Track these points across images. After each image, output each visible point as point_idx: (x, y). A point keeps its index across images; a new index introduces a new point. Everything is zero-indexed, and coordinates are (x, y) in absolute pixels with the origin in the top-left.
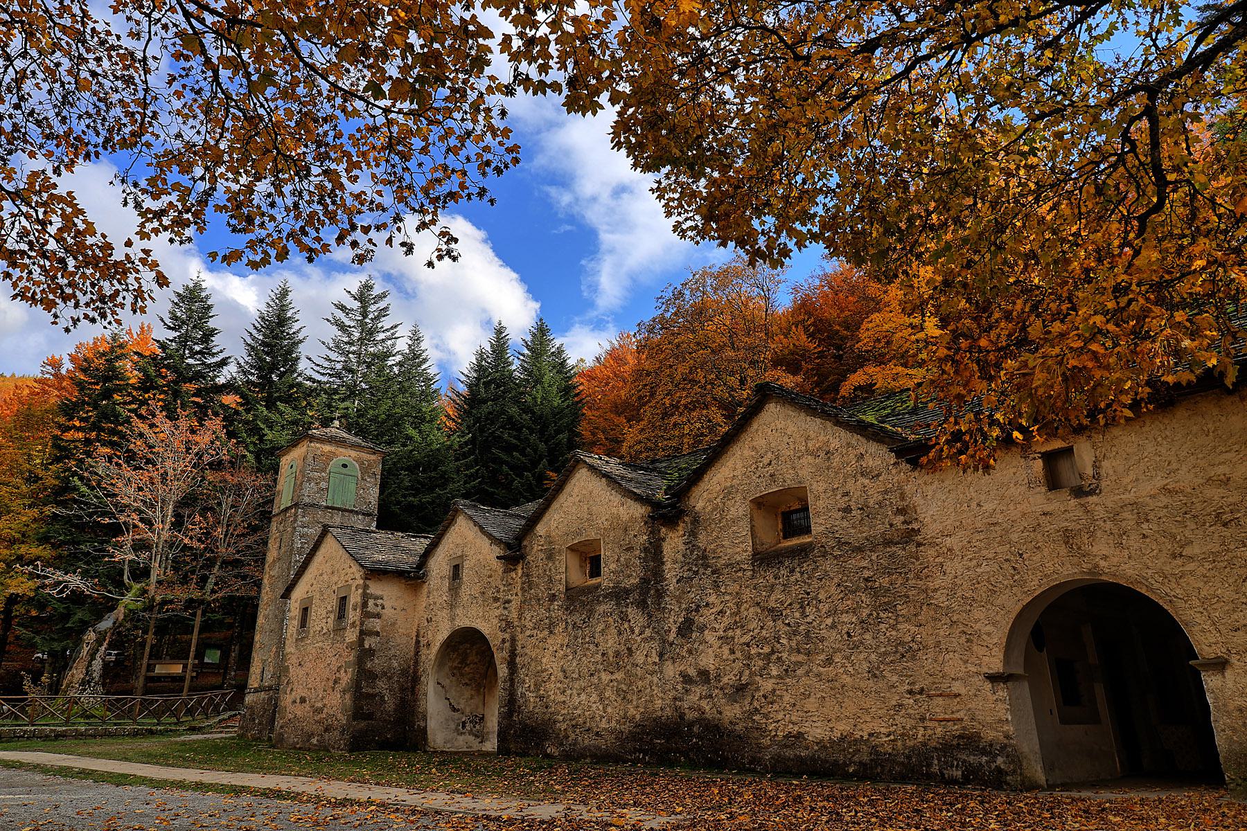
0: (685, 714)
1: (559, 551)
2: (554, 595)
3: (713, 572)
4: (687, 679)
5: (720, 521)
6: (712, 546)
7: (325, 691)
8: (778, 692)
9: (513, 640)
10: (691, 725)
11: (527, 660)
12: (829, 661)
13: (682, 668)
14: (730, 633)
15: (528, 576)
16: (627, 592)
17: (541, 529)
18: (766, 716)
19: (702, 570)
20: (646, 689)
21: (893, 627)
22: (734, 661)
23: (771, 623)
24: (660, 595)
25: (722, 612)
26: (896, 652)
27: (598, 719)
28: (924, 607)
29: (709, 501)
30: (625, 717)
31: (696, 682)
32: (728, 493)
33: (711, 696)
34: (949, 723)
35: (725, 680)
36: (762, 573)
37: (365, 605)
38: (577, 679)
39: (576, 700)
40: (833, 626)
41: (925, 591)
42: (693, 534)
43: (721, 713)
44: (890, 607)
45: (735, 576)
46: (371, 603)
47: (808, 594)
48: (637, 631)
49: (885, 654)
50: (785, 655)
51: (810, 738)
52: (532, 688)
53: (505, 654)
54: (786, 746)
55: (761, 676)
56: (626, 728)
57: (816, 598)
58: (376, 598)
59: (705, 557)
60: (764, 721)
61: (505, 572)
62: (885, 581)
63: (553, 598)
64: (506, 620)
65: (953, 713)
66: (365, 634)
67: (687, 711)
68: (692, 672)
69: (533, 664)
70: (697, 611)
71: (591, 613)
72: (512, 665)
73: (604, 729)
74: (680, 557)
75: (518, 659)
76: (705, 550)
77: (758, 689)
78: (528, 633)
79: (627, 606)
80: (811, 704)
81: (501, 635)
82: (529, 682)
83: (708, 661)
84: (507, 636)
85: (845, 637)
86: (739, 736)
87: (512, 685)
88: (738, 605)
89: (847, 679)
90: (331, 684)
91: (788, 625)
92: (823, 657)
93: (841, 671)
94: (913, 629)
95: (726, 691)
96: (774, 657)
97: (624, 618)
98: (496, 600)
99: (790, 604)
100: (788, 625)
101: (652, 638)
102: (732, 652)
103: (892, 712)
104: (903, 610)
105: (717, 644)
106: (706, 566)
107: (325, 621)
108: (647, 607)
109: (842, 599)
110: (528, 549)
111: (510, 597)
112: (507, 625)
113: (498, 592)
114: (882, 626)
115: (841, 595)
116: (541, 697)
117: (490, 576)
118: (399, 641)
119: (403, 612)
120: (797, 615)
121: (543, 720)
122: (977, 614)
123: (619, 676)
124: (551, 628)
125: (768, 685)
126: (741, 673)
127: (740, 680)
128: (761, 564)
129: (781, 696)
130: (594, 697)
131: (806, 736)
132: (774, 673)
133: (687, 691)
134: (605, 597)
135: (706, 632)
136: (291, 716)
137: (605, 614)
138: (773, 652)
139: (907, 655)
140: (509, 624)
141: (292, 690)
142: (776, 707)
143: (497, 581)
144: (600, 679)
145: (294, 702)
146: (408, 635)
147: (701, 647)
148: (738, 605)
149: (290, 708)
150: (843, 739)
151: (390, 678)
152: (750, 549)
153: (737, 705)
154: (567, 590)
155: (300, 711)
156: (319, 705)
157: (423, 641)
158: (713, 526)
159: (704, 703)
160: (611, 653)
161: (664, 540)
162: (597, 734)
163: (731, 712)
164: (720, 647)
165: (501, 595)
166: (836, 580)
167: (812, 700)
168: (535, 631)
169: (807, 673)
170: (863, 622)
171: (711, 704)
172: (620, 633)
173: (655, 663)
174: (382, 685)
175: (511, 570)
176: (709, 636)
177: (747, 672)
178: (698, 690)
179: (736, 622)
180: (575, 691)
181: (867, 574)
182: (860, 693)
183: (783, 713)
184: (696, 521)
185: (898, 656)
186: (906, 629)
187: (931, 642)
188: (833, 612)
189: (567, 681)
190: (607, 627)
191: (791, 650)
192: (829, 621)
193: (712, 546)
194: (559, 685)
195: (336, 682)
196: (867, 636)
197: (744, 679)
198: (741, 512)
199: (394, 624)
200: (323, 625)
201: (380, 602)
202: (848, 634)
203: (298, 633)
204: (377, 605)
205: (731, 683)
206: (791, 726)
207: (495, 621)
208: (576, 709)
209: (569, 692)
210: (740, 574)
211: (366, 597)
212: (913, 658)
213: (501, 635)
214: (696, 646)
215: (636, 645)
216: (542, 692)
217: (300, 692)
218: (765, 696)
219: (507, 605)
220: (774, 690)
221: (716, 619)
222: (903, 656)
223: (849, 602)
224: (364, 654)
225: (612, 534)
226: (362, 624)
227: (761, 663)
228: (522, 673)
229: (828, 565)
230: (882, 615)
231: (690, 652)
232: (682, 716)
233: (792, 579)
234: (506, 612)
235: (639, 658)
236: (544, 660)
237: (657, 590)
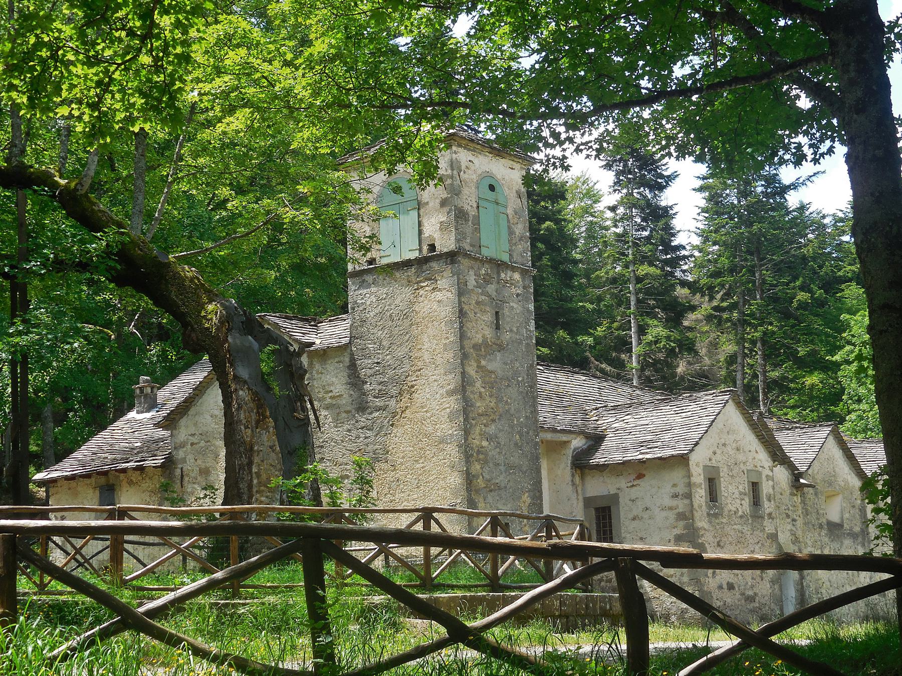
7: (753, 578)
82: (813, 587)
98: (788, 516)
113: (789, 510)
134: (848, 534)
145: (720, 587)
156: (751, 593)
165: (790, 513)
200: (738, 506)
203: (710, 508)
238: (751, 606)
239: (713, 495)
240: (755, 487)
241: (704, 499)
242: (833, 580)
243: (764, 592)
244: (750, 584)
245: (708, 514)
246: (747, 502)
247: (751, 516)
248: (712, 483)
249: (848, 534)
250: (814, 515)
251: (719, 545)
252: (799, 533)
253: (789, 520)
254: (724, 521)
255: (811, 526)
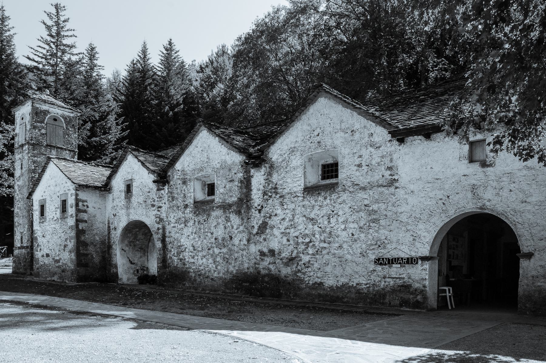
0: (260, 271)
1: (190, 180)
2: (187, 205)
3: (280, 197)
4: (262, 254)
5: (286, 168)
6: (281, 182)
7: (59, 251)
8: (311, 262)
9: (164, 228)
10: (265, 276)
11: (172, 239)
12: (340, 247)
13: (260, 248)
14: (288, 231)
15: (171, 193)
16: (230, 206)
17: (178, 166)
18: (304, 274)
19: (274, 195)
20: (239, 257)
21: (377, 231)
22: (289, 245)
23: (311, 226)
24: (249, 208)
25: (283, 219)
26: (376, 244)
27: (213, 272)
28: (394, 222)
29: (281, 155)
30: (228, 271)
31: (267, 256)
32: (292, 151)
33: (275, 263)
34: (398, 280)
35: (283, 255)
36: (308, 199)
37: (77, 205)
38: (201, 251)
39: (200, 262)
40: (345, 229)
41: (396, 213)
42: (270, 174)
43: (280, 271)
44: (374, 221)
45: (293, 199)
46: (80, 204)
47: (333, 211)
48: (235, 227)
49: (372, 245)
50: (317, 244)
51: (326, 285)
52: (176, 254)
53: (160, 236)
54: (313, 289)
55: (303, 253)
56: (228, 277)
57: (337, 214)
58: (83, 201)
59: (276, 188)
60: (303, 276)
61: (159, 190)
62: (375, 207)
63: (186, 206)
64: (159, 217)
65: (400, 275)
66: (79, 221)
67: (261, 270)
68: (265, 250)
69: (176, 242)
70: (270, 218)
71: (209, 215)
72: (163, 241)
73: (216, 277)
74: (261, 187)
75: (167, 239)
76: (276, 184)
77: (301, 260)
78: (172, 225)
79: (230, 213)
80: (328, 269)
81: (157, 226)
82: (174, 251)
83: (275, 245)
84: (160, 226)
85: (351, 235)
86: (289, 283)
87: (164, 253)
88: (293, 216)
89: (349, 257)
90: (63, 247)
91: (321, 227)
92: (337, 245)
93: (346, 252)
94: (387, 232)
95: (284, 261)
96: (311, 244)
97: (228, 220)
98: (153, 206)
99: (322, 217)
100: (321, 227)
101: (244, 231)
102: (288, 240)
103: (370, 274)
104: (382, 222)
105: (280, 236)
106: (276, 193)
107: (55, 213)
108: (242, 215)
109: (351, 215)
110: (171, 178)
111: (161, 205)
112: (161, 220)
113: (154, 201)
114: (371, 230)
115: (351, 213)
116: (181, 260)
117: (149, 192)
118: (98, 226)
119: (99, 210)
120: (326, 222)
121: (182, 272)
122: (421, 226)
123: (224, 250)
124: (186, 222)
125: (305, 258)
126: (292, 252)
127: (291, 255)
128: (308, 194)
129: (313, 264)
130: (211, 261)
131: (324, 284)
132: (311, 252)
133: (262, 260)
134: (217, 207)
135: (275, 229)
136: (42, 263)
137: (217, 217)
138: (311, 242)
139: (382, 246)
140: (161, 220)
141: (40, 249)
142: (310, 269)
143: (154, 194)
144: (214, 252)
145: (43, 256)
146: (103, 223)
147: (271, 238)
148: (293, 216)
149: (41, 259)
150: (343, 285)
151: (95, 246)
152: (303, 185)
153: (289, 268)
154: (195, 202)
155: (47, 261)
156: (57, 258)
157: (112, 227)
158: (282, 170)
159: (271, 267)
160: (220, 238)
161: (252, 177)
162: (212, 279)
163: (286, 271)
164: (282, 238)
165: (156, 203)
166: (349, 205)
167: (329, 266)
168: (177, 225)
169: (328, 253)
170: (361, 228)
171: (275, 267)
172: (225, 228)
173: (245, 245)
174: (91, 249)
175: (161, 189)
176: (276, 232)
177: (296, 251)
178: (268, 260)
179: (291, 225)
180: (199, 257)
181: (366, 202)
182: (354, 264)
183: (313, 272)
184: (272, 167)
185: (377, 246)
186: (383, 233)
187: (395, 240)
188: (345, 222)
189: (195, 252)
190: (218, 224)
191: (321, 241)
192: (343, 227)
193: (281, 182)
194: (190, 254)
195: (65, 246)
196: (362, 235)
197: (294, 255)
198: (299, 164)
199: (95, 216)
200: (54, 215)
201: (85, 204)
202: (353, 235)
203: (40, 219)
204: (84, 206)
205: (286, 256)
206: (317, 279)
207: (154, 217)
208: (201, 266)
209: (196, 257)
210: (296, 199)
211: (77, 201)
212: (385, 248)
213: (157, 226)
214: (268, 236)
215: (235, 235)
216: (181, 257)
217: (46, 251)
218: (304, 264)
219: (159, 209)
220: (310, 261)
221: (280, 223)
222: (379, 246)
223: (355, 217)
224: (80, 233)
225: (221, 172)
226: (77, 216)
227: (303, 247)
228: (169, 246)
229: (345, 196)
230: (371, 224)
231: (265, 240)
232: (259, 272)
233: (325, 203)
234: (159, 213)
235: (236, 241)
236: (182, 240)
237: (248, 206)
238: (57, 265)
239: (42, 213)
240: (64, 203)
241: (38, 217)
242: (196, 246)
243: (66, 257)
244: (57, 253)
245: (40, 223)
246: (59, 211)
247: (61, 219)
248: (42, 207)
249: (217, 207)
250: (180, 200)
251: (43, 236)
252: (164, 215)
253: (154, 208)
254: (47, 224)
255: (175, 208)
